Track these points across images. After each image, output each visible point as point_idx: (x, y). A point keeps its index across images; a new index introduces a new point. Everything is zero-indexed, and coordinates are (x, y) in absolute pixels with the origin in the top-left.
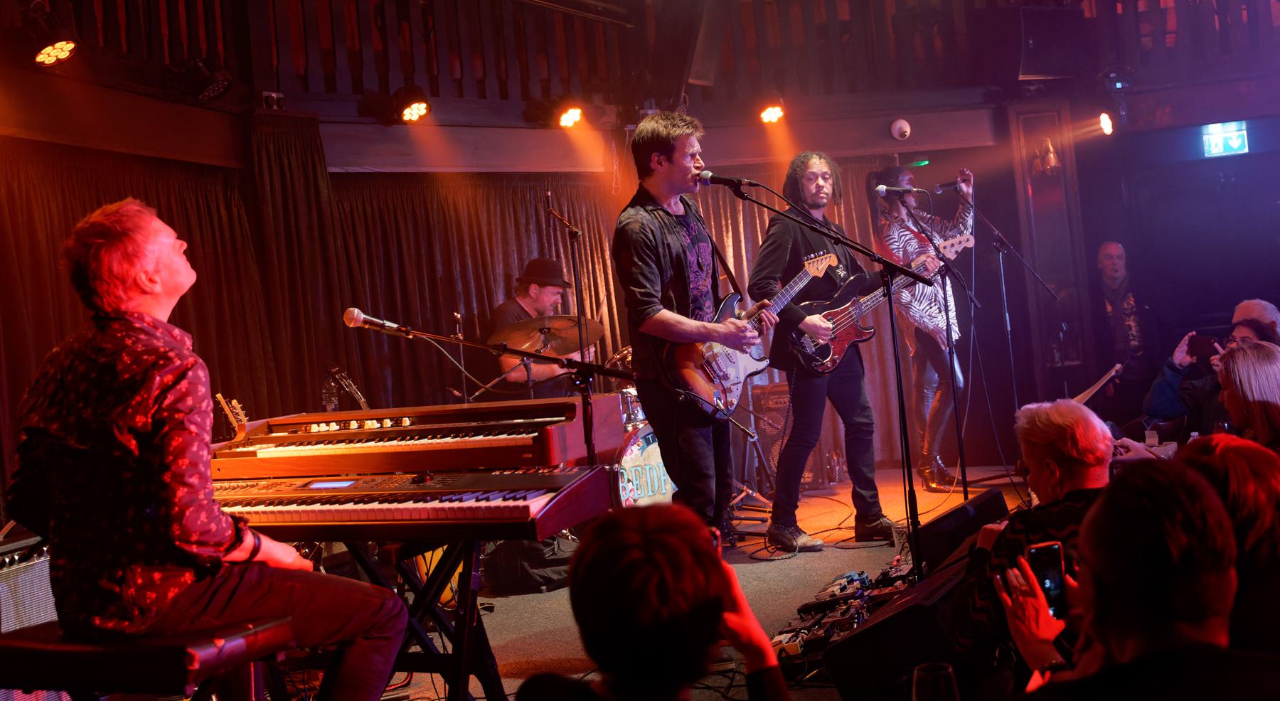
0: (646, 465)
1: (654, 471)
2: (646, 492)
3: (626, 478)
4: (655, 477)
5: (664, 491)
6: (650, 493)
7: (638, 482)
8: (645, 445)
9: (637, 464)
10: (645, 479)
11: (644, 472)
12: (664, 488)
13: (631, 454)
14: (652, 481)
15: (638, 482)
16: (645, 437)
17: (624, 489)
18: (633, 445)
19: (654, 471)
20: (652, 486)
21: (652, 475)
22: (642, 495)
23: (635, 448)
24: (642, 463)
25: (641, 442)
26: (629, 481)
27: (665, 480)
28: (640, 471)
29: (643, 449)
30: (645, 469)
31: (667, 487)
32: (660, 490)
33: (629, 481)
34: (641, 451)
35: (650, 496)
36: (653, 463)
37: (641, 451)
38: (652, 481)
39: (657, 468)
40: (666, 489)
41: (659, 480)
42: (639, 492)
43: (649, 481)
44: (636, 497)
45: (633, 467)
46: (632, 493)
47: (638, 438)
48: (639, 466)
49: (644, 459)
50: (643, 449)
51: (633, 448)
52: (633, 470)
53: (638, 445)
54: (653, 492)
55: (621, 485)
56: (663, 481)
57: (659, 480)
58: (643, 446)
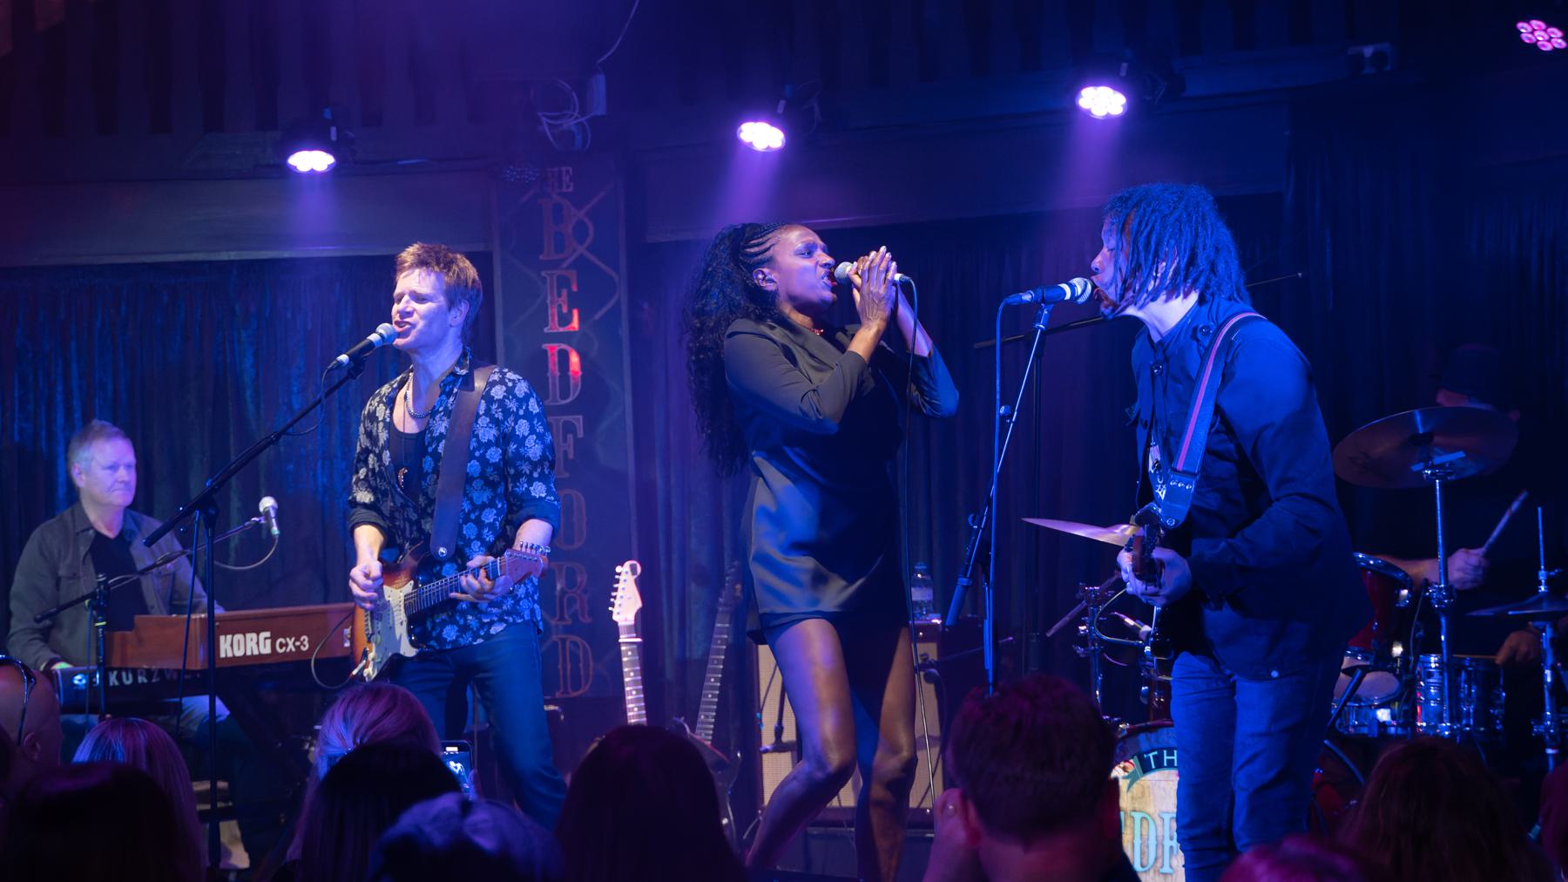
0: (1135, 811)
1: (1151, 822)
4: (1152, 843)
5: (1166, 869)
8: (1139, 771)
11: (1128, 822)
19: (1151, 822)
20: (1142, 853)
21: (1144, 833)
25: (1132, 765)
27: (1171, 847)
29: (1133, 778)
30: (1133, 818)
32: (1159, 865)
36: (1151, 810)
37: (1128, 781)
39: (1159, 822)
40: (1171, 867)
41: (1160, 845)
47: (1125, 755)
49: (1133, 798)
53: (1124, 769)
54: (1142, 866)
57: (1160, 845)
58: (1134, 772)
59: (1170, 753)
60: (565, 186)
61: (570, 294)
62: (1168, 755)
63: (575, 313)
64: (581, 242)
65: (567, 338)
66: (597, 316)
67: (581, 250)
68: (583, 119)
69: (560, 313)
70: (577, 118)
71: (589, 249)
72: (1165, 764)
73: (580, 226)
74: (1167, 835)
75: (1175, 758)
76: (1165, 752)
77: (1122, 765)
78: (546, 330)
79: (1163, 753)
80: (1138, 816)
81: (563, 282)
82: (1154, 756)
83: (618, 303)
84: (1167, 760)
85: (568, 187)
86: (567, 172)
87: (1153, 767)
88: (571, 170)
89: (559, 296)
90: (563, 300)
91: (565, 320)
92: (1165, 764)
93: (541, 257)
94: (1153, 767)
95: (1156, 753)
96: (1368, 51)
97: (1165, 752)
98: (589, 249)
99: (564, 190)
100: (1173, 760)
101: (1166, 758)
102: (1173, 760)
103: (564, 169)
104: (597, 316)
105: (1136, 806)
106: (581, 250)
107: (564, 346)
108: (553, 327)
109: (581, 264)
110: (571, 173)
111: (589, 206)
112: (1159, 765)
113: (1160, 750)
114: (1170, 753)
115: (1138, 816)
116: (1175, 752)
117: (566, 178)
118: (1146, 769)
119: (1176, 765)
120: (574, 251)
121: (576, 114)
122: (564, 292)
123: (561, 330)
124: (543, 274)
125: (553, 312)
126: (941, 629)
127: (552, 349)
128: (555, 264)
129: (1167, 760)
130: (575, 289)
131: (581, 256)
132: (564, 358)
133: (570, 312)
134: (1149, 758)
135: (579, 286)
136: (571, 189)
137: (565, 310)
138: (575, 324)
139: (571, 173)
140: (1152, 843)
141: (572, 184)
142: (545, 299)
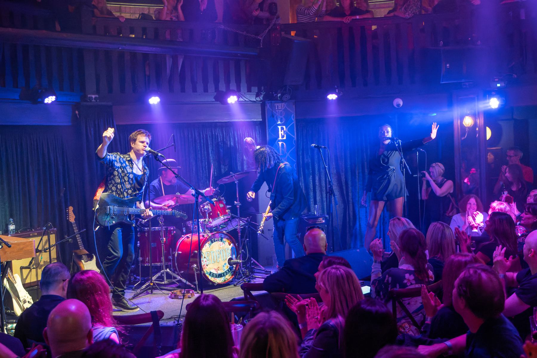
2: (211, 262)
3: (203, 256)
5: (218, 261)
6: (213, 262)
7: (208, 258)
9: (208, 251)
10: (211, 257)
11: (210, 254)
12: (218, 260)
13: (205, 247)
14: (214, 257)
15: (208, 258)
16: (211, 240)
17: (203, 261)
18: (206, 243)
22: (210, 263)
23: (207, 244)
24: (209, 250)
26: (205, 257)
28: (209, 253)
29: (210, 245)
31: (219, 259)
33: (205, 257)
34: (209, 245)
35: (213, 263)
36: (214, 250)
37: (209, 245)
38: (214, 257)
39: (216, 252)
42: (209, 262)
43: (212, 257)
44: (207, 264)
45: (206, 252)
46: (206, 262)
48: (208, 252)
50: (210, 245)
51: (206, 244)
52: (206, 253)
53: (208, 243)
55: (202, 259)
56: (218, 258)
57: (216, 257)
74: (218, 255)
77: (208, 242)
80: (212, 252)
96: (93, 96)
101: (215, 239)
105: (211, 250)
112: (215, 241)
113: (214, 238)
115: (212, 252)
118: (212, 242)
140: (215, 256)
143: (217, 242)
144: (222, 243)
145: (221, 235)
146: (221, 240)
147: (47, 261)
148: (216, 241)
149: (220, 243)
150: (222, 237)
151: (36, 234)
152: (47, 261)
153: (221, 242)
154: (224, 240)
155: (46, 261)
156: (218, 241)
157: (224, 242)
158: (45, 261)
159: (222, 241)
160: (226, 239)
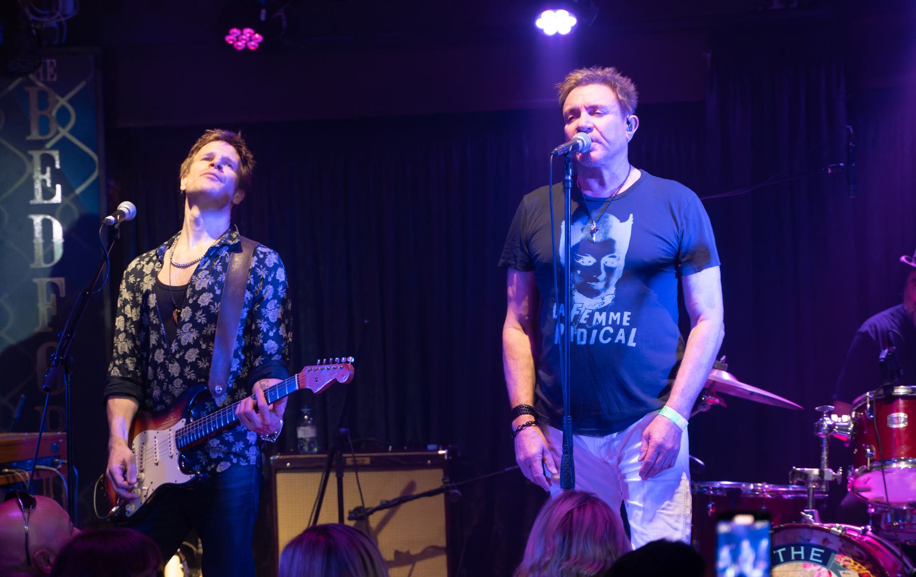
59: (798, 549)
60: (49, 76)
61: (54, 170)
62: (795, 550)
63: (58, 187)
64: (64, 126)
65: (50, 209)
66: (78, 191)
67: (64, 132)
68: (63, 19)
69: (44, 189)
70: (59, 18)
71: (72, 132)
72: (793, 558)
73: (63, 112)
75: (802, 552)
76: (793, 548)
78: (32, 202)
79: (791, 549)
81: (47, 161)
82: (782, 552)
83: (98, 179)
84: (796, 555)
85: (52, 76)
86: (52, 63)
87: (782, 560)
88: (54, 61)
89: (44, 172)
90: (47, 176)
91: (48, 193)
92: (793, 558)
93: (29, 138)
94: (782, 560)
95: (784, 549)
97: (793, 548)
98: (72, 132)
99: (49, 79)
100: (800, 555)
101: (793, 553)
102: (800, 555)
103: (48, 61)
104: (78, 191)
106: (64, 132)
107: (49, 217)
108: (38, 198)
109: (62, 146)
110: (55, 64)
111: (71, 95)
112: (787, 558)
113: (788, 547)
114: (798, 549)
116: (802, 548)
117: (50, 70)
119: (803, 557)
120: (58, 132)
121: (59, 14)
122: (48, 169)
123: (46, 202)
124: (30, 152)
125: (38, 186)
126: (446, 457)
127: (38, 220)
128: (39, 145)
129: (796, 555)
130: (58, 166)
131: (64, 139)
132: (47, 226)
133: (54, 187)
134: (778, 554)
135: (61, 164)
136: (55, 79)
137: (49, 184)
138: (57, 198)
139: (55, 64)
141: (56, 76)
142: (31, 175)
143: (800, 564)
144: (824, 570)
145: (825, 540)
146: (825, 560)
147: (408, 552)
148: (798, 558)
149: (814, 568)
150: (830, 546)
151: (367, 461)
152: (408, 552)
153: (819, 567)
154: (841, 560)
155: (404, 550)
156: (807, 558)
157: (836, 569)
158: (400, 550)
159: (825, 564)
160: (847, 558)
